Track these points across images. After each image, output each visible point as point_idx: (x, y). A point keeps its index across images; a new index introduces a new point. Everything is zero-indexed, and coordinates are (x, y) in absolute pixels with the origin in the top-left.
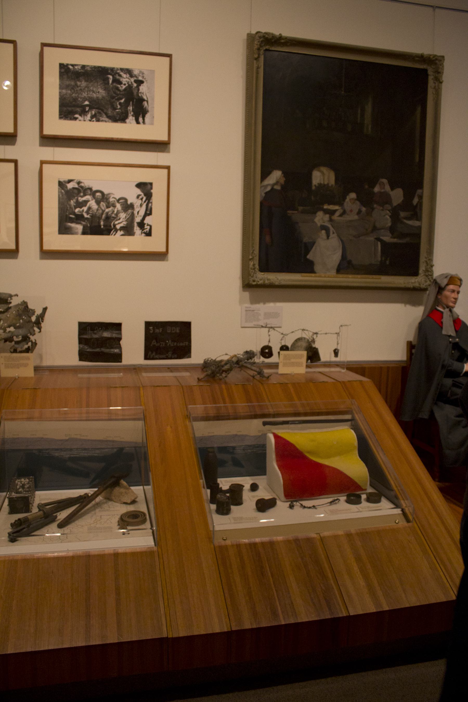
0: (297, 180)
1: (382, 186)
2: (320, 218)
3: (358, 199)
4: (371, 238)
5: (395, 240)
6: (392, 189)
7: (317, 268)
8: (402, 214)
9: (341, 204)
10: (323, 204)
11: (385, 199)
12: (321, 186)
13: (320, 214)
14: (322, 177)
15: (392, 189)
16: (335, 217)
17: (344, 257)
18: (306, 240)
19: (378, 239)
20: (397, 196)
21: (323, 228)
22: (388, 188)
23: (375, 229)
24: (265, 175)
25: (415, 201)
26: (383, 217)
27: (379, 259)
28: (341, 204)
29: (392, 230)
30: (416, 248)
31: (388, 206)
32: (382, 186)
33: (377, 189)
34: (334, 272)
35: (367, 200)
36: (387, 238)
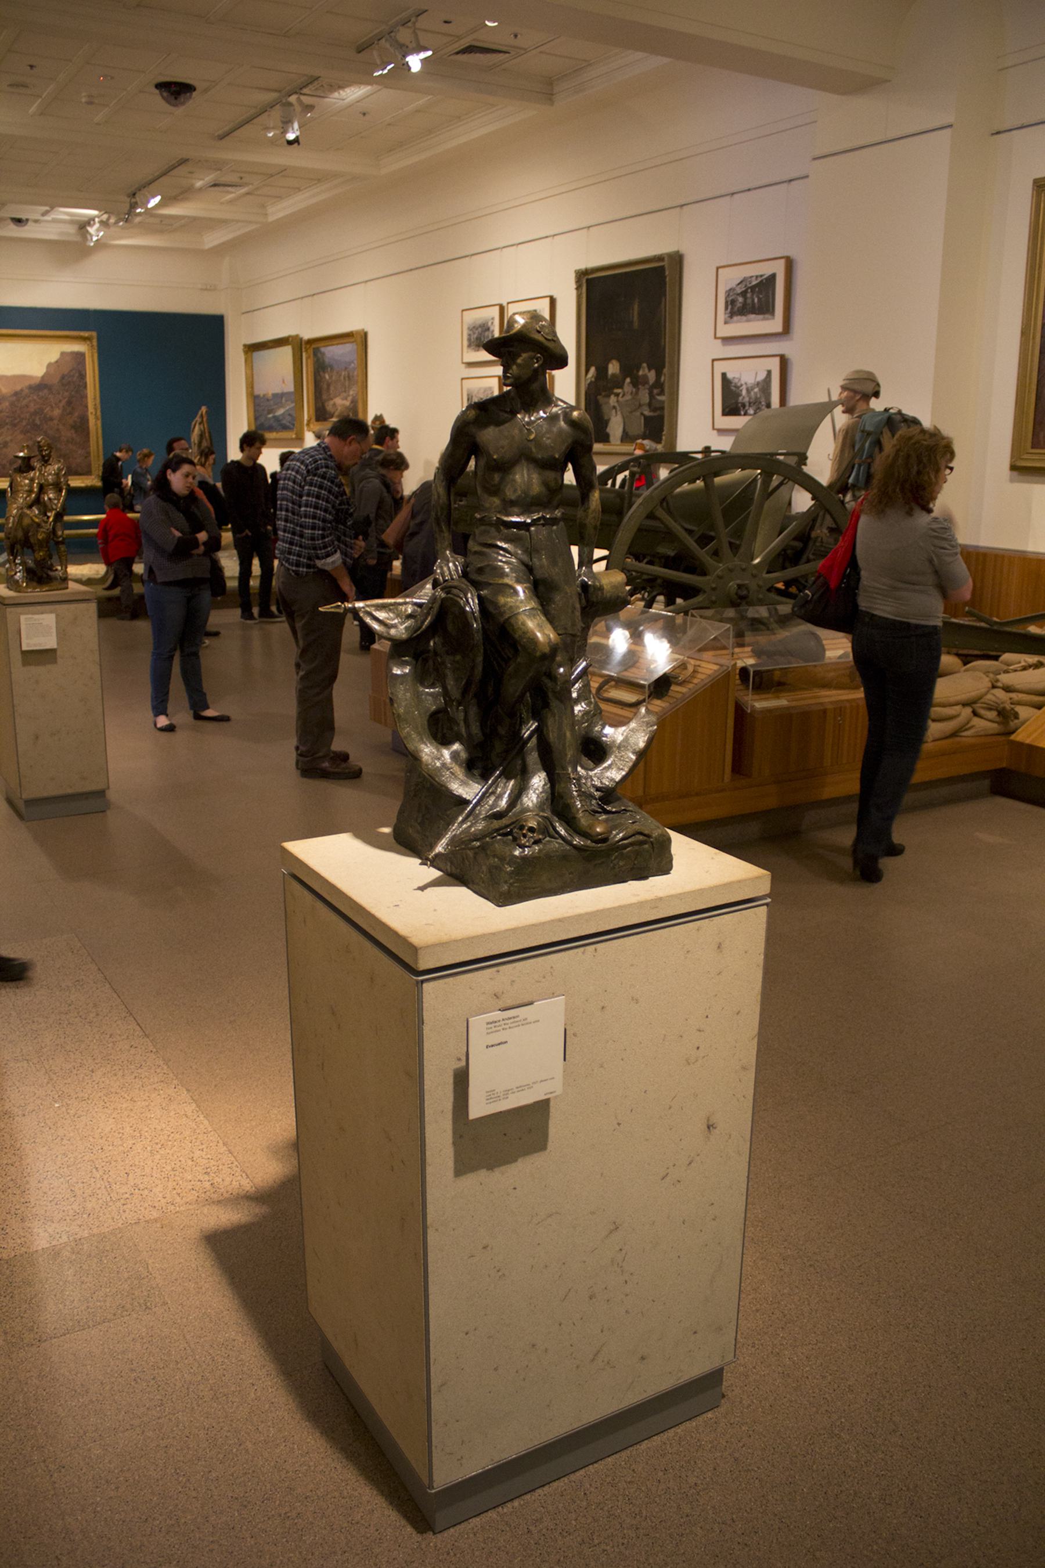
0: (602, 371)
1: (644, 371)
2: (613, 400)
3: (632, 382)
4: (638, 414)
5: (651, 414)
6: (650, 370)
7: (611, 438)
8: (655, 391)
9: (621, 387)
10: (613, 388)
11: (645, 380)
12: (613, 375)
13: (612, 397)
14: (613, 368)
15: (650, 370)
16: (620, 399)
17: (624, 430)
18: (606, 418)
19: (642, 414)
20: (652, 376)
21: (614, 407)
22: (646, 370)
23: (640, 405)
24: (587, 371)
25: (663, 379)
26: (644, 396)
27: (642, 429)
28: (621, 387)
29: (650, 405)
30: (661, 418)
31: (647, 386)
32: (644, 371)
33: (641, 373)
34: (619, 442)
35: (635, 383)
36: (647, 413)
